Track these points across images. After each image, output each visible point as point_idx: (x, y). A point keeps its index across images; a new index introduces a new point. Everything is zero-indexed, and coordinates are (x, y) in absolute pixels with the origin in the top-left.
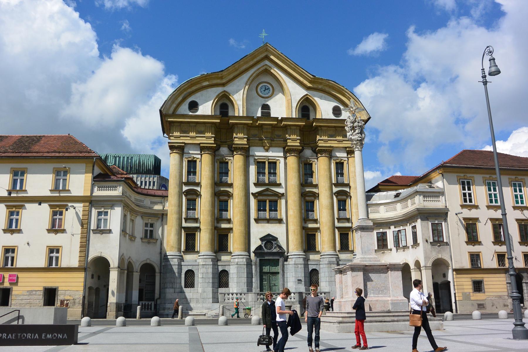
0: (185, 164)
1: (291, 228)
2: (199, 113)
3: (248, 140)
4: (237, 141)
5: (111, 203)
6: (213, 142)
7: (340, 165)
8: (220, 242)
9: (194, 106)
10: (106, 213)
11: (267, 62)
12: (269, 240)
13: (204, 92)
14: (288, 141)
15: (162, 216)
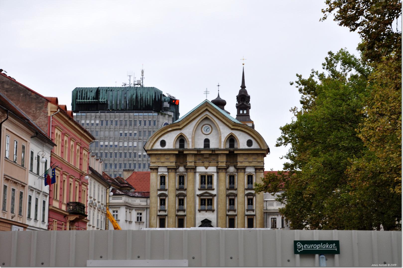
0: (159, 178)
1: (219, 215)
2: (166, 147)
3: (195, 162)
4: (189, 164)
5: (119, 206)
6: (174, 165)
7: (250, 177)
9: (163, 143)
10: (117, 212)
11: (207, 113)
13: (169, 134)
14: (219, 163)
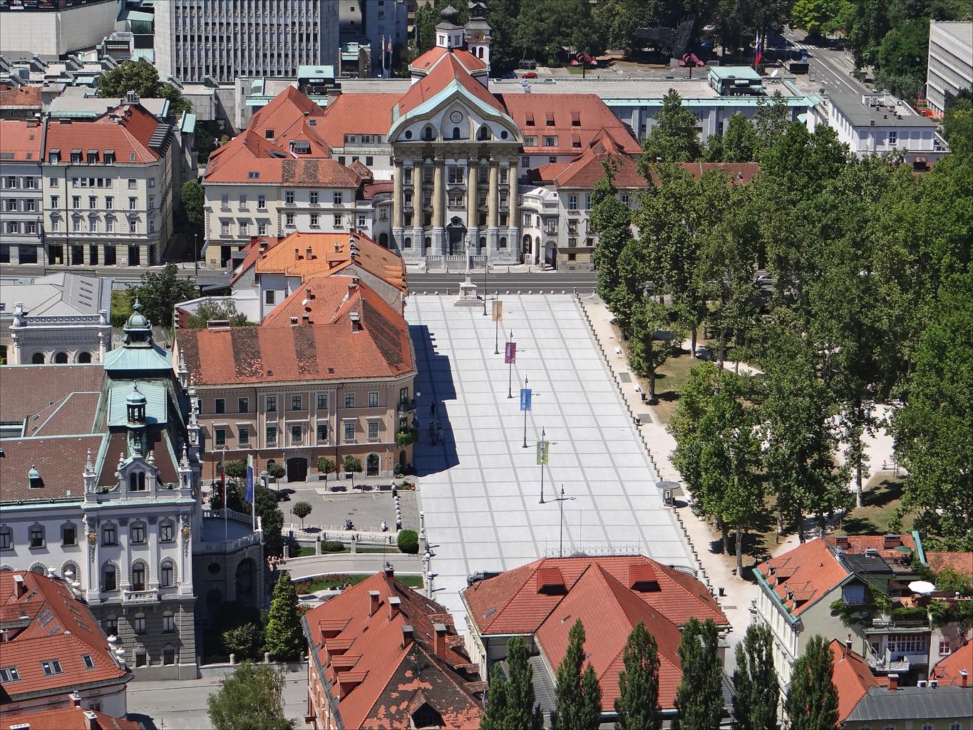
8: (426, 221)
9: (409, 134)
12: (456, 220)
15: (391, 205)
